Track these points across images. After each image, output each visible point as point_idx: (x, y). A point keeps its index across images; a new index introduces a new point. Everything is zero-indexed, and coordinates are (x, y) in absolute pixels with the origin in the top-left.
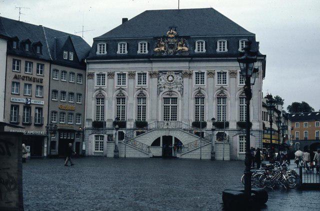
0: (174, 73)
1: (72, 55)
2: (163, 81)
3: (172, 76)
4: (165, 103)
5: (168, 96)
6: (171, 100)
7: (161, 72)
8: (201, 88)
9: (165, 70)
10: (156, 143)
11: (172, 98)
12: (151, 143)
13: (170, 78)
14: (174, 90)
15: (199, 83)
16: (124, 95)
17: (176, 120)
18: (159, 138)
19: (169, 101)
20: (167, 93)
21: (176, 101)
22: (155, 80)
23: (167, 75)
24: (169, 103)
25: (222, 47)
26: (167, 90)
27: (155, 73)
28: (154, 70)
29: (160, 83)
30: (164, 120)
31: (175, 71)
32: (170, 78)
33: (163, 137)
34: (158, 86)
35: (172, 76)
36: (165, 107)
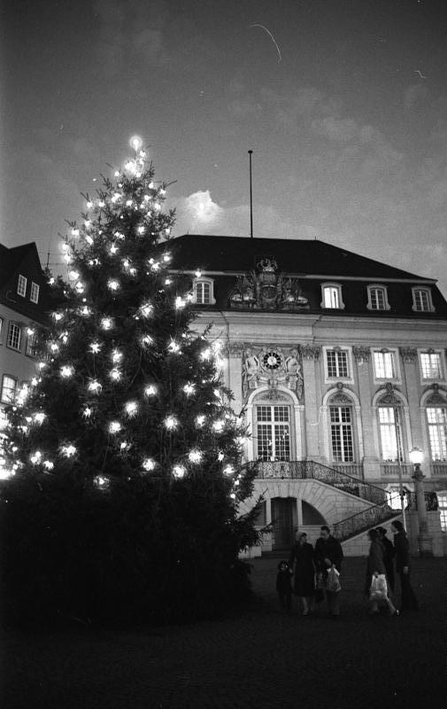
1: (36, 289)
3: (277, 356)
4: (259, 419)
5: (266, 403)
9: (259, 341)
13: (272, 361)
14: (281, 388)
20: (267, 394)
24: (270, 419)
25: (378, 296)
26: (265, 388)
29: (250, 371)
31: (281, 345)
32: (272, 361)
34: (243, 378)
35: (277, 356)
36: (259, 427)
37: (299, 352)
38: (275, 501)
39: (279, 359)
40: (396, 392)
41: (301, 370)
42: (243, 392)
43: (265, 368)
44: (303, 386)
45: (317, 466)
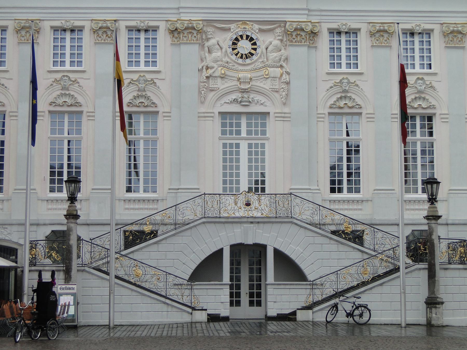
0: (256, 27)
2: (217, 54)
6: (244, 121)
7: (209, 22)
8: (349, 82)
10: (207, 269)
11: (249, 114)
12: (190, 272)
15: (340, 65)
16: (78, 104)
17: (263, 190)
18: (220, 252)
19: (238, 125)
20: (234, 96)
21: (264, 125)
22: (190, 51)
23: (231, 36)
27: (190, 29)
28: (184, 17)
29: (209, 61)
30: (225, 189)
33: (232, 247)
35: (252, 39)
37: (287, 33)
38: (237, 250)
39: (255, 44)
40: (429, 91)
41: (286, 59)
42: (200, 93)
43: (234, 57)
44: (288, 83)
45: (298, 200)
